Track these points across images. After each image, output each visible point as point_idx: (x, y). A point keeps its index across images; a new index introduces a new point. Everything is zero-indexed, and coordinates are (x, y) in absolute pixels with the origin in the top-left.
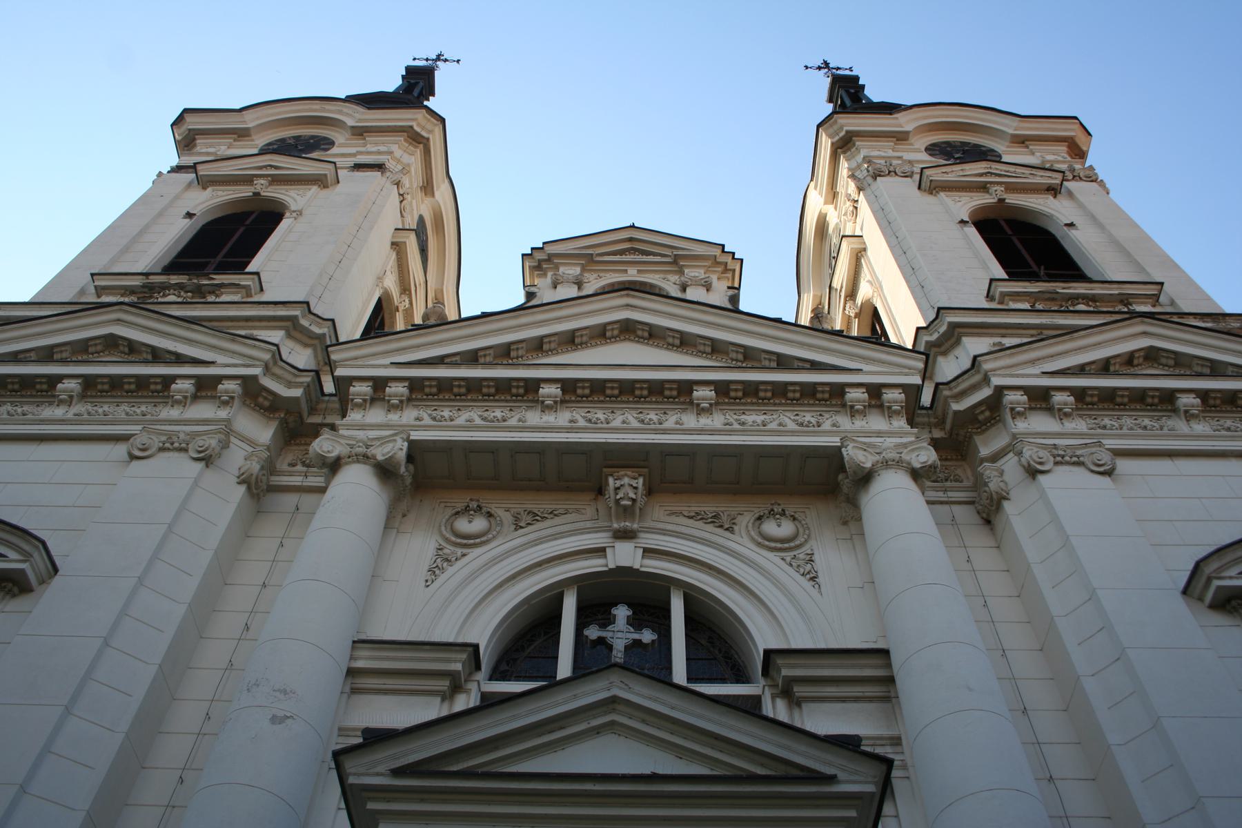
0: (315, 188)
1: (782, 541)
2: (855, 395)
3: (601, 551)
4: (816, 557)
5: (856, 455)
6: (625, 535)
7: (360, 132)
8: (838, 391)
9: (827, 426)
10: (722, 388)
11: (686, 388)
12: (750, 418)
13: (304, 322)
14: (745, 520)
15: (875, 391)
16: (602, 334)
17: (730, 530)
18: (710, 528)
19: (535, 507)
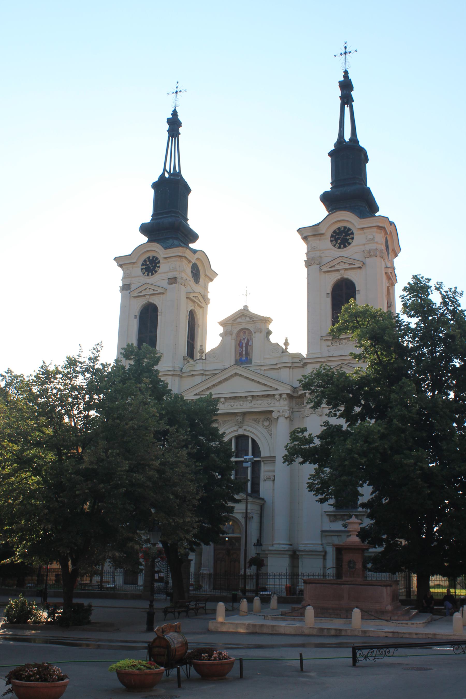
0: (161, 295)
1: (268, 426)
2: (277, 396)
3: (237, 430)
4: (273, 430)
5: (275, 415)
6: (240, 427)
7: (166, 258)
8: (274, 395)
9: (272, 404)
10: (252, 396)
11: (246, 397)
12: (259, 402)
13: (175, 373)
14: (261, 420)
15: (281, 395)
16: (232, 376)
17: (259, 423)
18: (255, 422)
19: (225, 419)
